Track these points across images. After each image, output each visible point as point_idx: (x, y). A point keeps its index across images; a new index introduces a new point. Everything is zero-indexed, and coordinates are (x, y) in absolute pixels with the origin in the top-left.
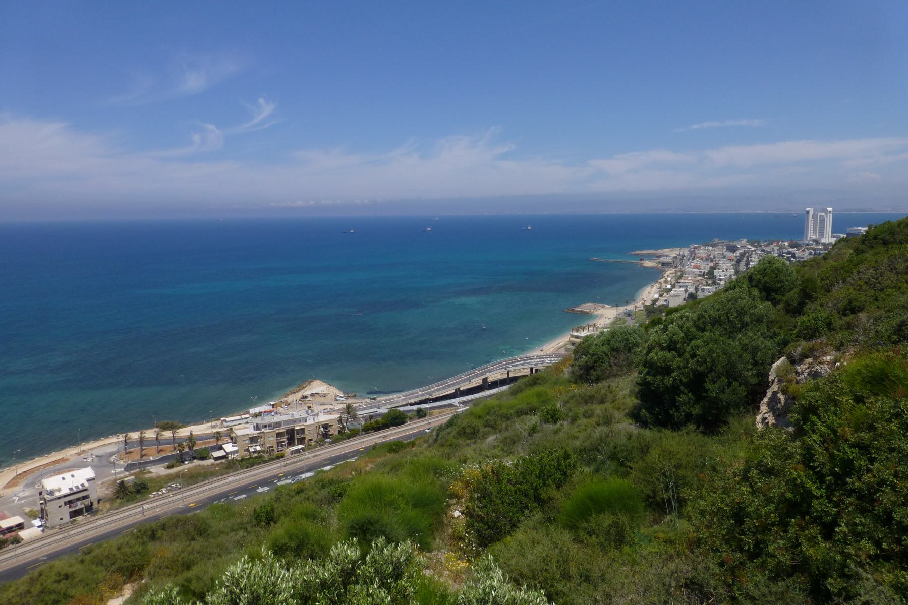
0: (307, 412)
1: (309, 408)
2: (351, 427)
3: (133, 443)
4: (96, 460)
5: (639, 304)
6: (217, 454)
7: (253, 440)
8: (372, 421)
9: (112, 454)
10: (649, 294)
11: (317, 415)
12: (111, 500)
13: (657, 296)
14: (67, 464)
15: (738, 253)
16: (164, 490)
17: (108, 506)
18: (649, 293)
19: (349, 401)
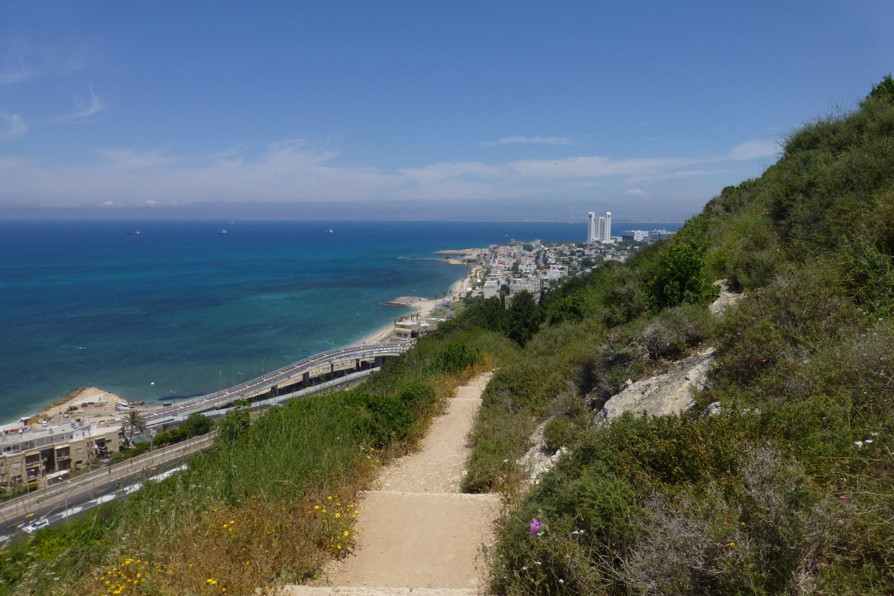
1: (79, 420)
2: (138, 441)
8: (167, 431)
10: (462, 287)
11: (88, 428)
13: (470, 289)
15: (534, 251)
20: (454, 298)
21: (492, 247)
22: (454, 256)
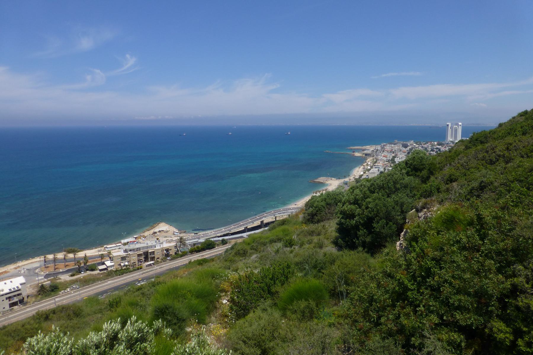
0: (156, 242)
1: (158, 239)
2: (183, 250)
3: (50, 261)
4: (26, 272)
5: (352, 178)
6: (101, 267)
7: (123, 258)
8: (195, 247)
9: (36, 268)
10: (358, 172)
11: (162, 243)
12: (36, 296)
13: (362, 173)
14: (8, 274)
16: (68, 290)
17: (34, 299)
18: (358, 171)
19: (182, 235)
20: (350, 179)
21: (382, 145)
22: (358, 150)
